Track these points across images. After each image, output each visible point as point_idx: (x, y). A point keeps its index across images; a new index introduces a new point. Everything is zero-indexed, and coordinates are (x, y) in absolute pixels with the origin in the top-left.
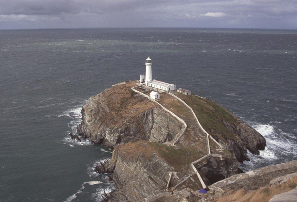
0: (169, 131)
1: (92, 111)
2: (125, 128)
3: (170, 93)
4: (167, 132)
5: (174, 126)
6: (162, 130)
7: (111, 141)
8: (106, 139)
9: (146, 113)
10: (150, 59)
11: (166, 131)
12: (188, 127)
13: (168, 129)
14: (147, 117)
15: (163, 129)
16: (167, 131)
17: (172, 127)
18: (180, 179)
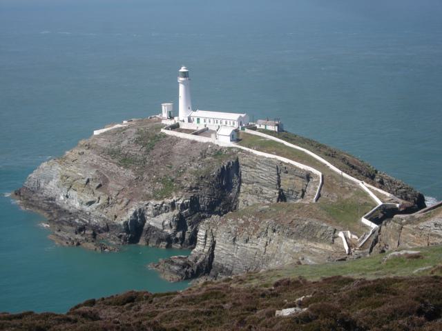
0: (281, 191)
1: (88, 181)
2: (191, 199)
3: (247, 131)
4: (278, 191)
5: (291, 179)
6: (264, 191)
7: (163, 226)
8: (150, 227)
9: (225, 166)
12: (323, 176)
13: (280, 187)
15: (265, 190)
16: (277, 189)
17: (287, 182)
18: (359, 238)
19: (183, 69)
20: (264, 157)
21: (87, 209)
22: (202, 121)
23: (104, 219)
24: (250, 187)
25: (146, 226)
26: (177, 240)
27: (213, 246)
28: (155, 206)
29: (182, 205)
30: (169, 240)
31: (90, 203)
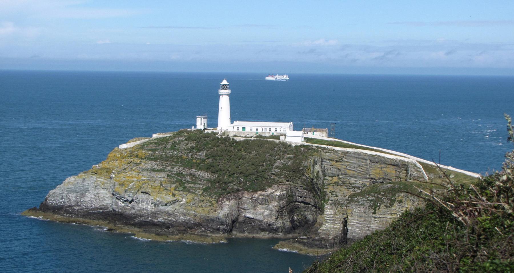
0: (372, 179)
7: (264, 217)
10: (228, 84)
11: (364, 180)
14: (313, 166)
15: (353, 180)
16: (367, 178)
19: (225, 82)
20: (348, 152)
21: (170, 209)
22: (248, 129)
23: (195, 215)
24: (335, 179)
25: (241, 219)
26: (278, 228)
27: (345, 223)
28: (251, 198)
29: (279, 196)
30: (270, 228)
31: (173, 202)
